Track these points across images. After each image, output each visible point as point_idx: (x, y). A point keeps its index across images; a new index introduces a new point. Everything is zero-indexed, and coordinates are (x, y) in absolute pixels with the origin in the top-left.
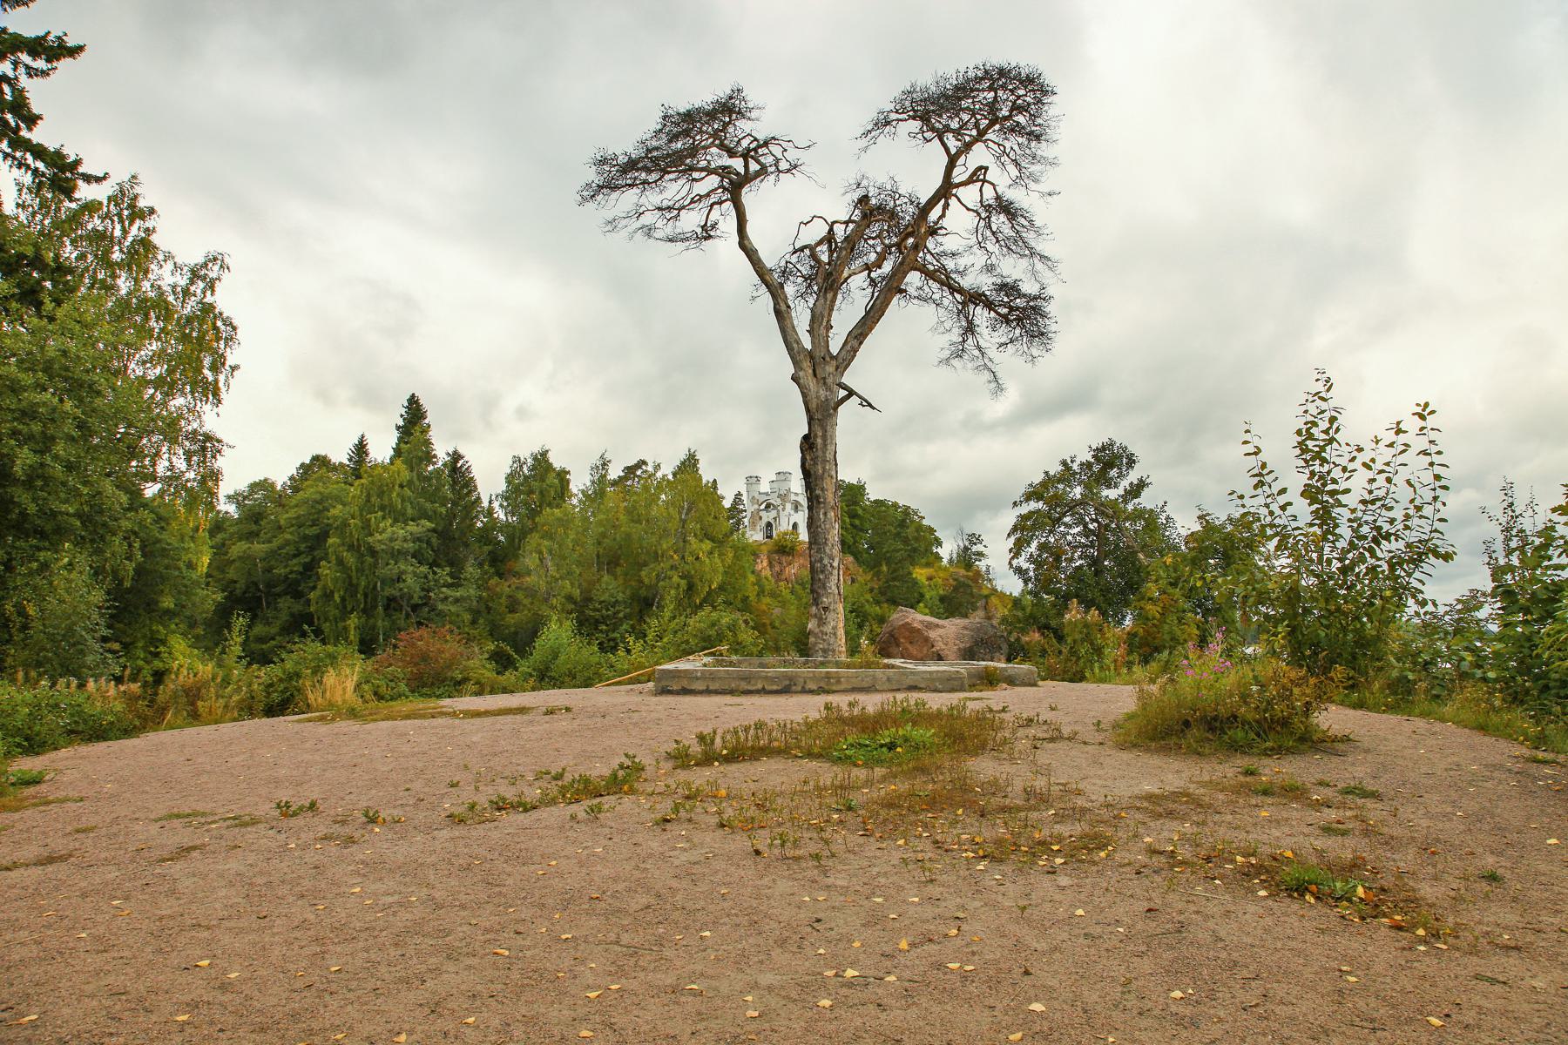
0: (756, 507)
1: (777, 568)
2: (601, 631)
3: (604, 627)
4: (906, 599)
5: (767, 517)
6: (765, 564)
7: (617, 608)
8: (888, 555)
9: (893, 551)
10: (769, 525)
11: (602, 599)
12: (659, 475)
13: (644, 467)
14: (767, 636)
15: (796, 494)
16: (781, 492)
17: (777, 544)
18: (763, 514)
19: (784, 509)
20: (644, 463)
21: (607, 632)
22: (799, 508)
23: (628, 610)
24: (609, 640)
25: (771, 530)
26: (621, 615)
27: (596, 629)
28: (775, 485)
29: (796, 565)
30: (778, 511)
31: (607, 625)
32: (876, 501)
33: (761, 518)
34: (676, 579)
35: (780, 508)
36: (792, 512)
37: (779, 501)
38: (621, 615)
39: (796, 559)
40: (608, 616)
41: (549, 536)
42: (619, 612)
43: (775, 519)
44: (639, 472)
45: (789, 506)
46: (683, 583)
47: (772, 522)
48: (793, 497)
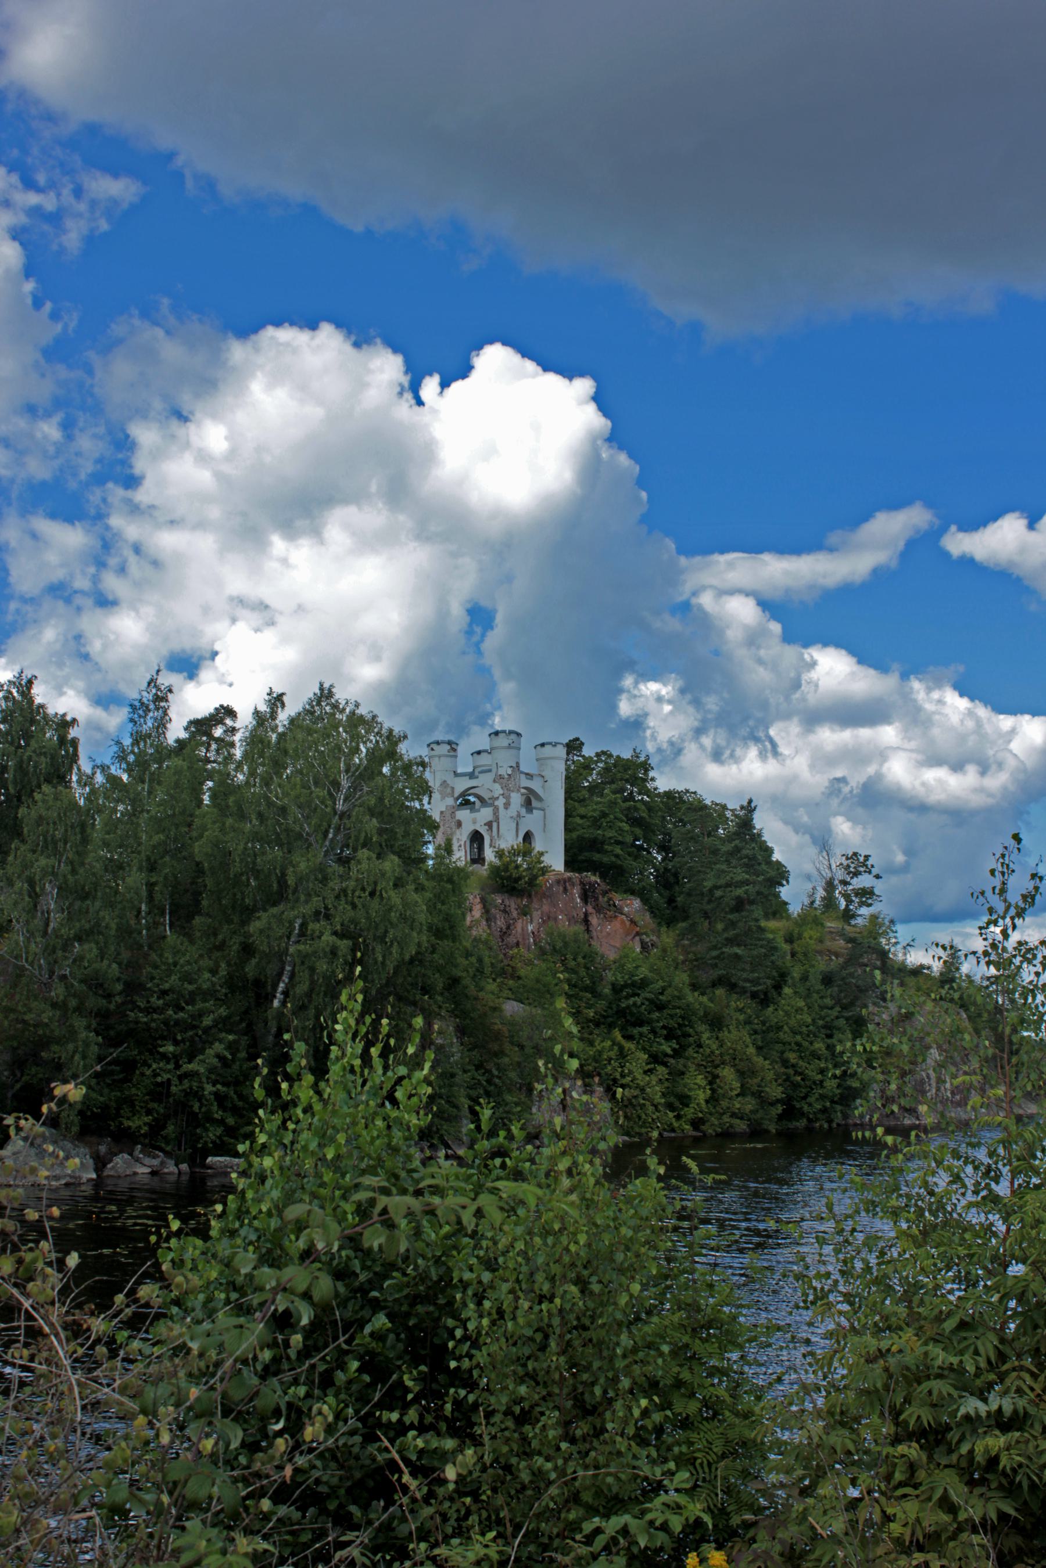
0: (450, 801)
1: (501, 923)
2: (164, 1056)
3: (171, 1048)
4: (755, 982)
5: (471, 820)
6: (477, 912)
7: (200, 1005)
8: (718, 893)
9: (728, 885)
10: (476, 838)
11: (167, 986)
12: (283, 717)
13: (229, 722)
14: (506, 1060)
15: (529, 776)
16: (502, 771)
17: (495, 871)
18: (463, 815)
19: (507, 806)
20: (230, 712)
21: (176, 1059)
22: (535, 803)
23: (223, 1011)
24: (181, 1078)
25: (481, 848)
26: (207, 1021)
27: (153, 1052)
28: (484, 760)
29: (536, 915)
30: (496, 810)
31: (176, 1043)
32: (669, 795)
33: (459, 824)
34: (328, 938)
35: (500, 803)
36: (523, 811)
37: (498, 790)
38: (207, 1021)
39: (535, 905)
40: (177, 1023)
41: (50, 846)
42: (201, 1015)
43: (489, 824)
44: (218, 732)
45: (517, 799)
46: (344, 945)
47: (483, 831)
48: (525, 782)
